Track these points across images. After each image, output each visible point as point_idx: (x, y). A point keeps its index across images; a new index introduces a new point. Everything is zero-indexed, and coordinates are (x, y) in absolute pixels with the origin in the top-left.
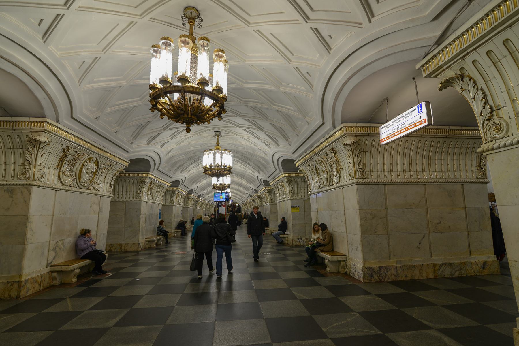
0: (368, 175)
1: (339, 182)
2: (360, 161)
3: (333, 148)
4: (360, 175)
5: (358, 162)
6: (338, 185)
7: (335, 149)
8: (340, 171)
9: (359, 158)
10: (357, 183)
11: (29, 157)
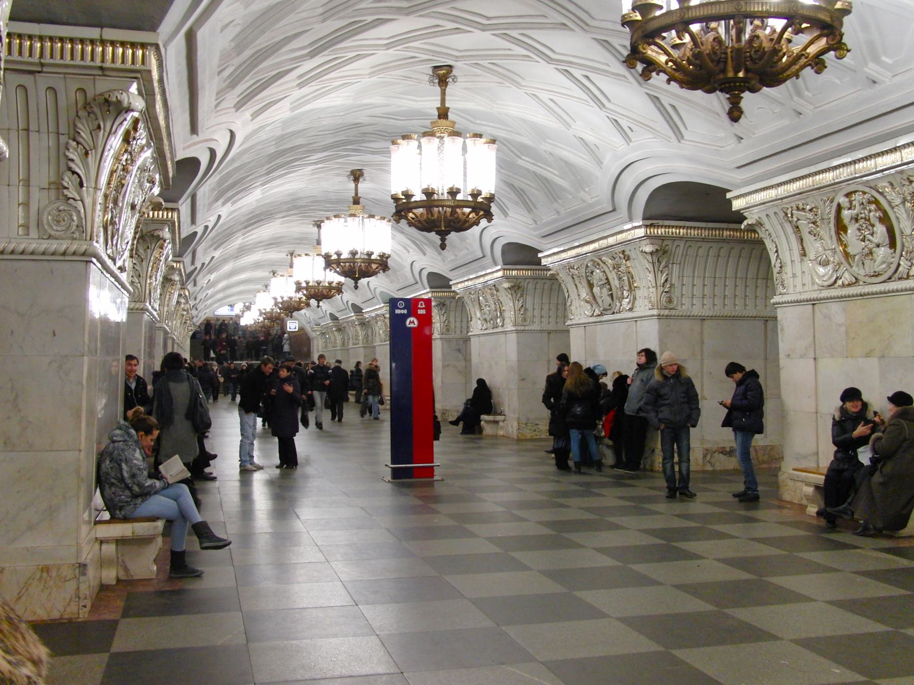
0: (677, 303)
1: (631, 310)
2: (666, 281)
3: (624, 251)
4: (664, 304)
5: (662, 282)
6: (629, 315)
7: (626, 253)
8: (634, 290)
9: (664, 275)
10: (659, 317)
11: (139, 265)
